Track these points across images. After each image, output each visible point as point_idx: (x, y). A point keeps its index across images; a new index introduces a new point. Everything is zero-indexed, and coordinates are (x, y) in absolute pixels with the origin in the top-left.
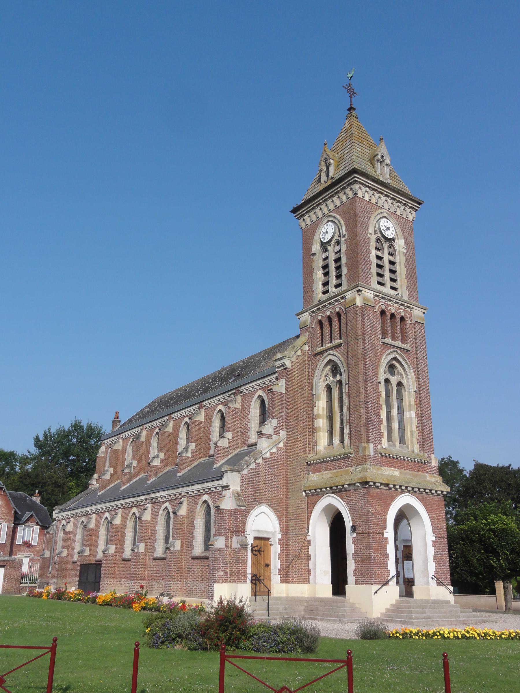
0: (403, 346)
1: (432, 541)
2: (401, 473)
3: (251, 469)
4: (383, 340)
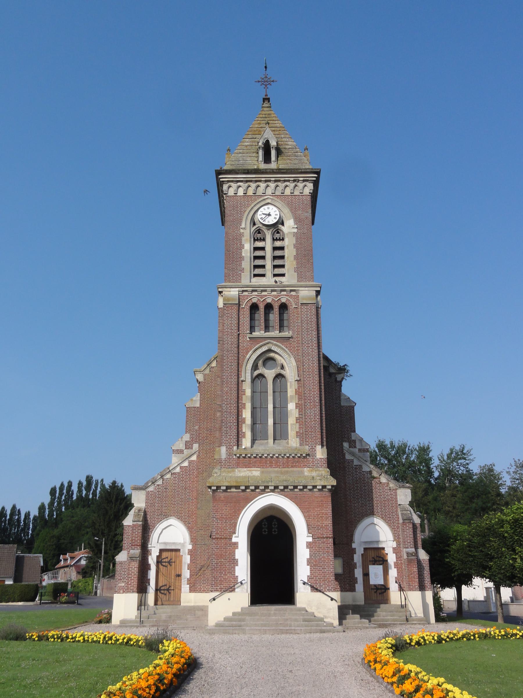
0: (283, 334)
1: (307, 542)
2: (262, 472)
3: (158, 485)
4: (251, 336)
